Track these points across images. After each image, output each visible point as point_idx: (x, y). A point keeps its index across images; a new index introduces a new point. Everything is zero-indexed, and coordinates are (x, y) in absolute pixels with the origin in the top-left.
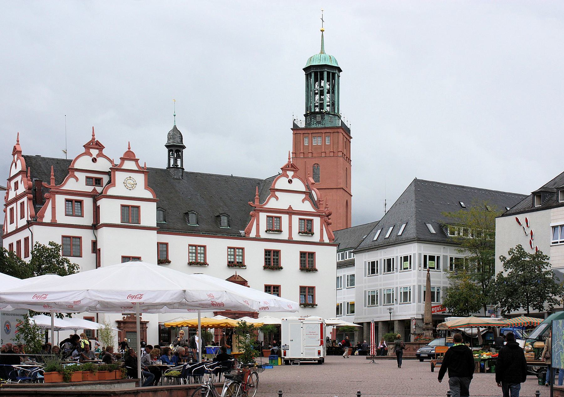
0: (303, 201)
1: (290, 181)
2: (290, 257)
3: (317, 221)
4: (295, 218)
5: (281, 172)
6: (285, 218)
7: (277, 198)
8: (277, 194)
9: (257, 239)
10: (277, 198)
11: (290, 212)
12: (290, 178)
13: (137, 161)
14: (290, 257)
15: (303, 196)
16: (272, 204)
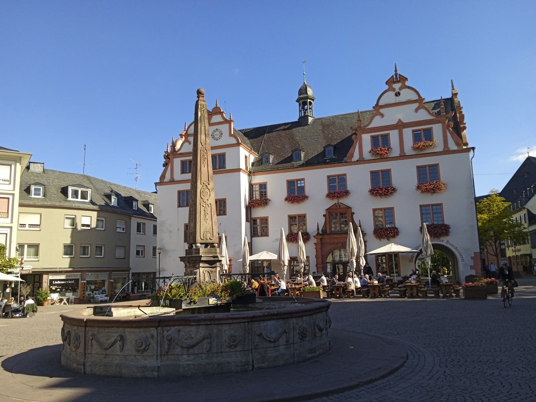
0: (416, 110)
1: (398, 94)
2: (404, 174)
3: (437, 130)
4: (408, 133)
5: (387, 87)
6: (394, 135)
7: (382, 115)
8: (382, 111)
9: (361, 161)
10: (382, 115)
11: (400, 126)
12: (397, 90)
13: (221, 113)
14: (404, 174)
15: (416, 105)
16: (378, 122)
